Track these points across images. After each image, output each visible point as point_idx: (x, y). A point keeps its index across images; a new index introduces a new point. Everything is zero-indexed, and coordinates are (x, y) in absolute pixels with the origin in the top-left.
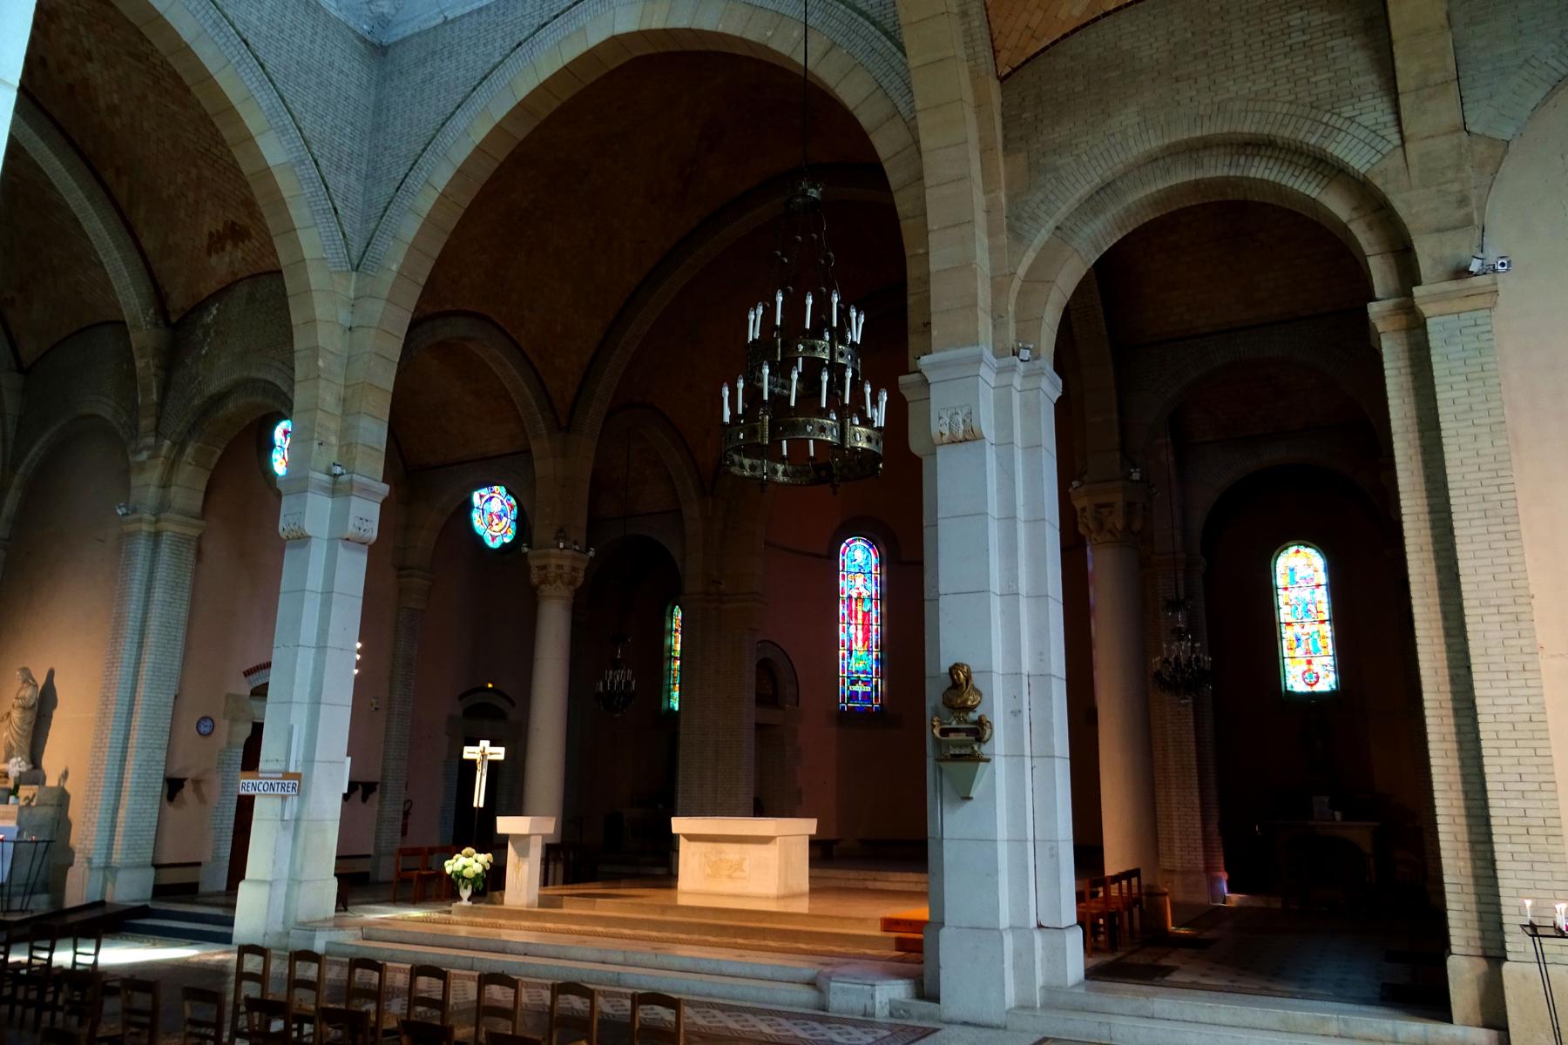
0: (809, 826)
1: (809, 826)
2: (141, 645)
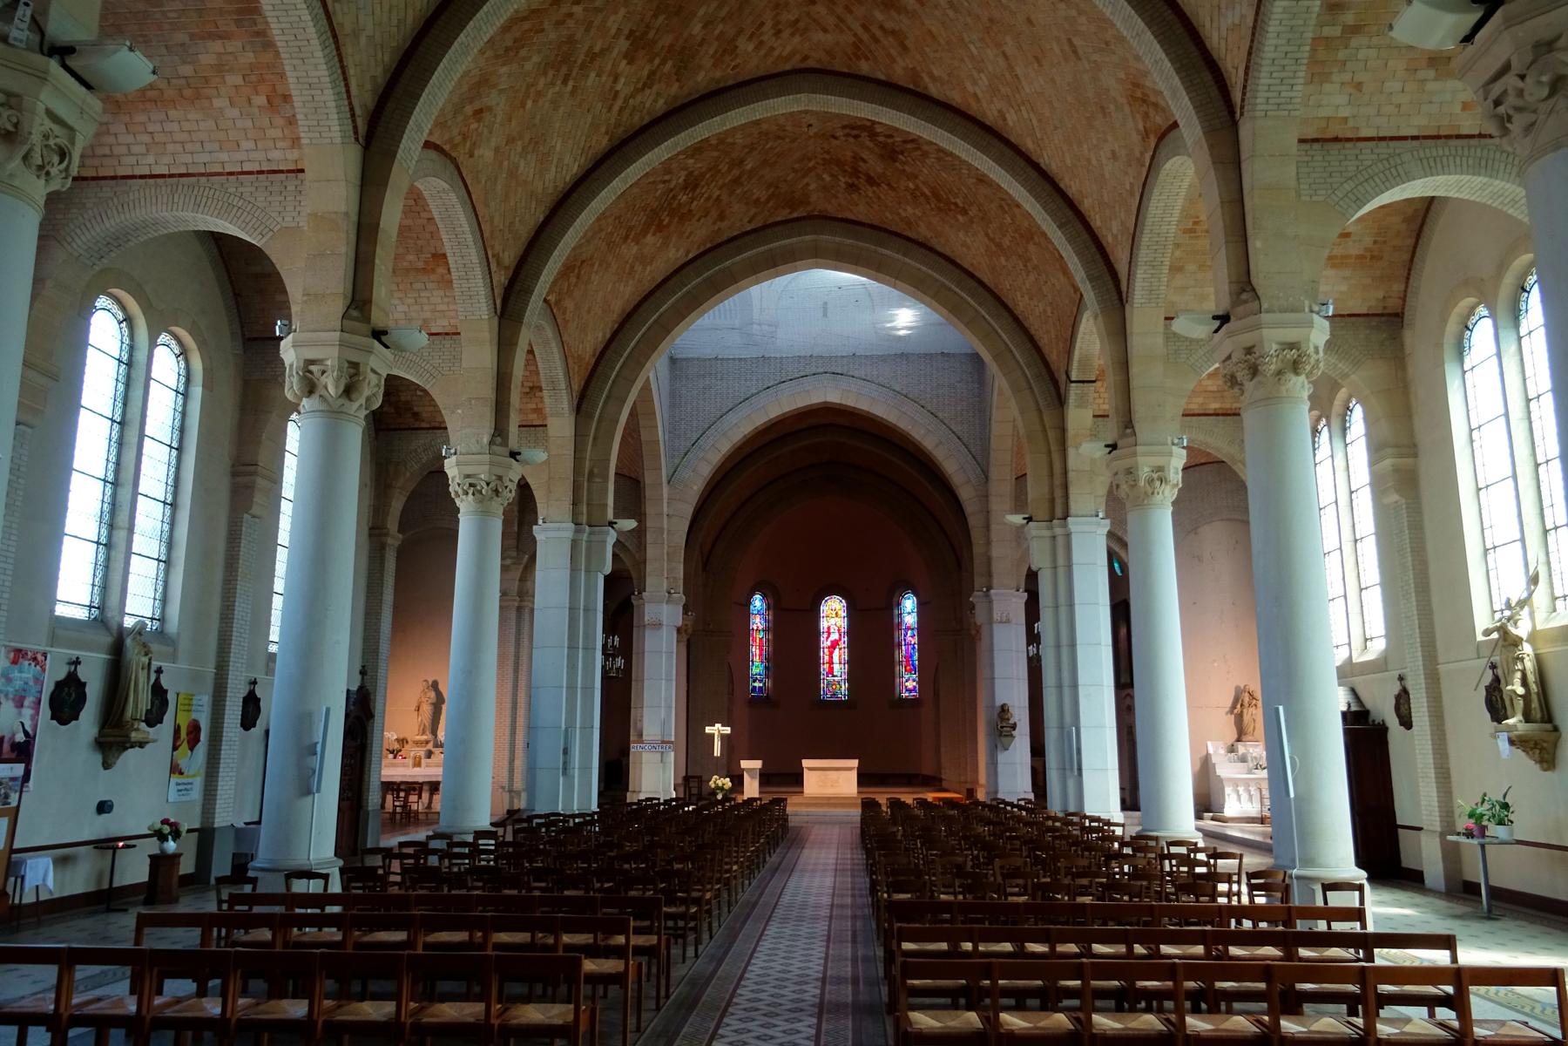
0: (855, 763)
1: (855, 763)
2: (516, 671)
